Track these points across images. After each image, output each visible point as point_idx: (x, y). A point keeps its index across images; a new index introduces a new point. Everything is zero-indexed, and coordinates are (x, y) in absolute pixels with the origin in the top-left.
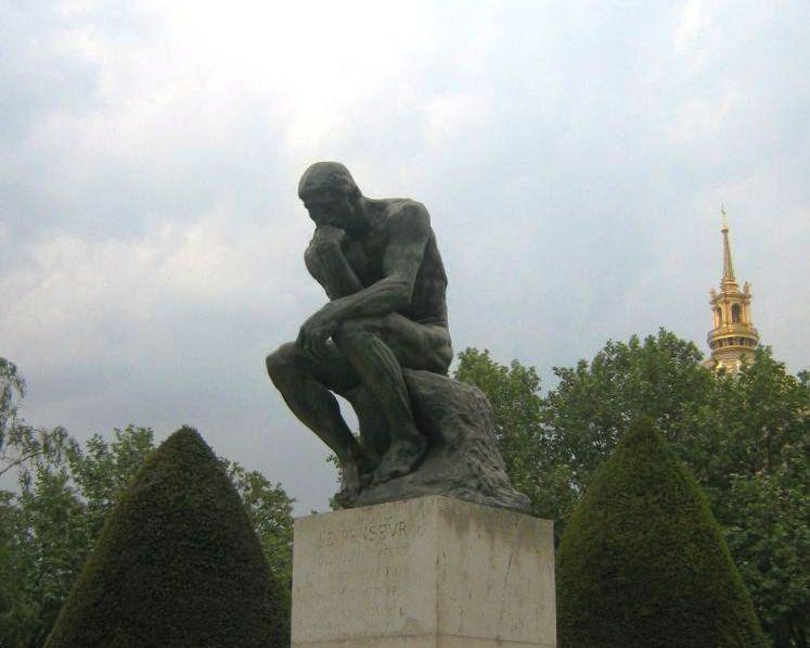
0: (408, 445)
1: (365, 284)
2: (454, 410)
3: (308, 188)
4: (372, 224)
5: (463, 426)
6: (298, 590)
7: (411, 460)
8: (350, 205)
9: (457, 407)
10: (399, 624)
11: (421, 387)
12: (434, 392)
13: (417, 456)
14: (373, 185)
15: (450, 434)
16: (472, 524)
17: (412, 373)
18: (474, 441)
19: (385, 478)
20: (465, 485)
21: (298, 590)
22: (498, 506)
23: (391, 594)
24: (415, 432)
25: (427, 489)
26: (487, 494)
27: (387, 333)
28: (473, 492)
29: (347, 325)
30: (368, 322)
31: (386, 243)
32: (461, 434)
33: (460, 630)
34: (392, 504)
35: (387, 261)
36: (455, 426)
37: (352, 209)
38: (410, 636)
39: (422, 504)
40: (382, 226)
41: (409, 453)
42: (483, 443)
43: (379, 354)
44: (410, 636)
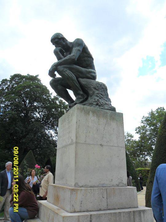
0: (80, 96)
2: (92, 86)
5: (94, 90)
7: (81, 100)
8: (62, 42)
9: (93, 86)
12: (86, 83)
13: (82, 99)
14: (70, 38)
15: (91, 92)
16: (91, 113)
17: (81, 79)
18: (98, 93)
20: (92, 104)
22: (103, 109)
24: (81, 93)
26: (100, 106)
27: (71, 69)
28: (95, 106)
29: (59, 67)
30: (63, 66)
32: (94, 92)
33: (85, 142)
36: (91, 90)
37: (64, 43)
41: (80, 98)
42: (101, 94)
43: (67, 73)
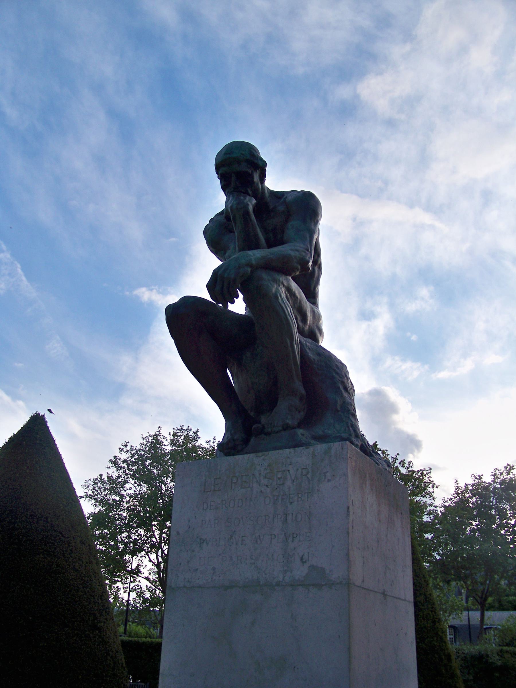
1: (270, 245)
2: (337, 376)
3: (228, 156)
4: (271, 207)
6: (178, 533)
10: (300, 572)
11: (308, 350)
12: (316, 358)
19: (277, 429)
21: (178, 533)
23: (291, 539)
25: (313, 442)
31: (287, 221)
34: (292, 450)
35: (290, 232)
38: (313, 585)
39: (330, 449)
40: (281, 208)
44: (313, 585)
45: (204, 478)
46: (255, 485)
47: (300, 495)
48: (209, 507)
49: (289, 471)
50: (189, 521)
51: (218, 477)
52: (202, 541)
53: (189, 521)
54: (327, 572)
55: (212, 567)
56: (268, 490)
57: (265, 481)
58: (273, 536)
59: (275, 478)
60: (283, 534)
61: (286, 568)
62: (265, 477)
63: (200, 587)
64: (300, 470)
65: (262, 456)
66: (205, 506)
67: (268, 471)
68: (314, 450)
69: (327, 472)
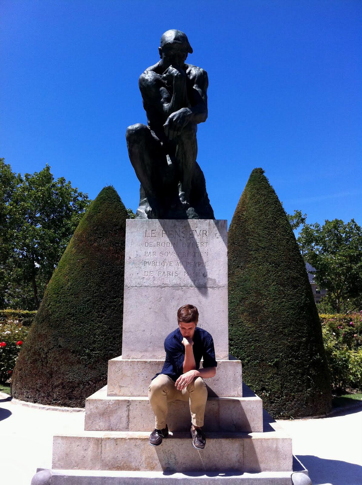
21: (130, 258)
23: (197, 265)
45: (145, 229)
46: (177, 236)
47: (202, 244)
48: (149, 245)
49: (196, 231)
50: (137, 251)
51: (154, 229)
52: (145, 263)
53: (137, 251)
54: (217, 281)
55: (153, 276)
56: (185, 239)
57: (183, 235)
58: (188, 263)
59: (188, 234)
60: (193, 262)
61: (195, 279)
62: (182, 233)
63: (145, 286)
64: (202, 232)
65: (180, 221)
66: (147, 244)
67: (184, 230)
68: (210, 222)
69: (216, 234)
